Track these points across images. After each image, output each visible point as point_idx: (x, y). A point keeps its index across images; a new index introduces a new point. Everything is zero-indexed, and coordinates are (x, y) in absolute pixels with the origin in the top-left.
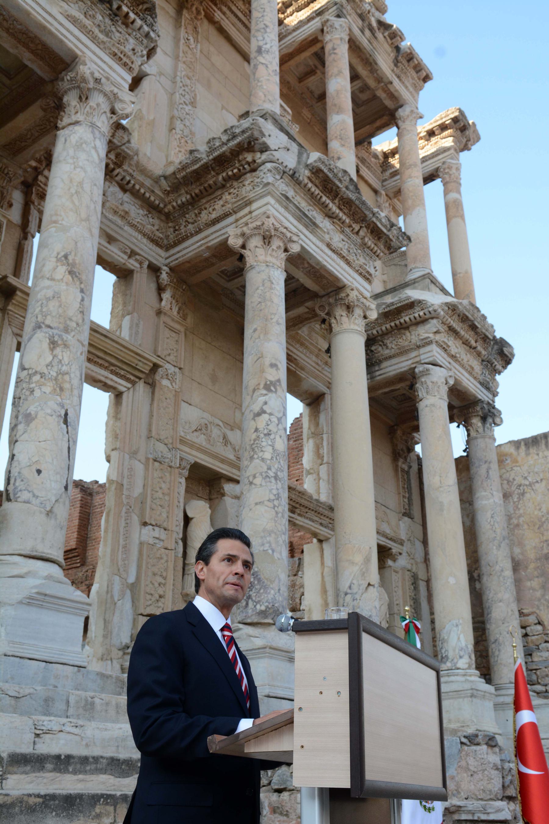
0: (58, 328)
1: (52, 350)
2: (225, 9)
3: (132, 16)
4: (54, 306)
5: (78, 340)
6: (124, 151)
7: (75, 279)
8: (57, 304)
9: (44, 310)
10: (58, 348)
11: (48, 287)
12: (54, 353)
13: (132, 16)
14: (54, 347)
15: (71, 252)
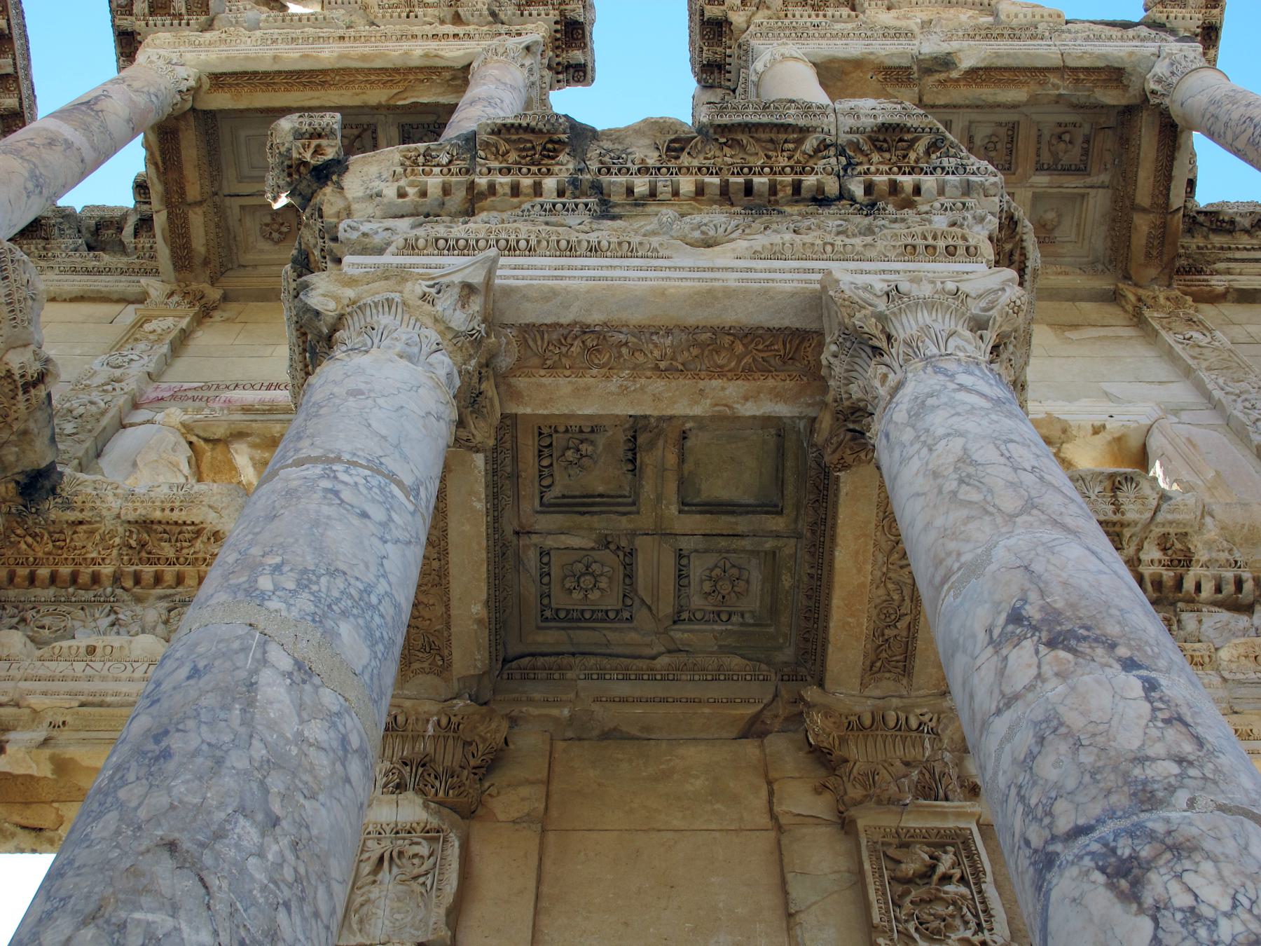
0: (1111, 814)
1: (1132, 897)
2: (1221, 266)
3: (907, 180)
4: (1057, 764)
5: (1222, 808)
6: (1171, 523)
7: (1083, 647)
8: (1063, 748)
9: (1033, 801)
10: (1152, 876)
11: (1012, 730)
12: (1148, 901)
13: (907, 180)
14: (1137, 883)
15: (1025, 600)
